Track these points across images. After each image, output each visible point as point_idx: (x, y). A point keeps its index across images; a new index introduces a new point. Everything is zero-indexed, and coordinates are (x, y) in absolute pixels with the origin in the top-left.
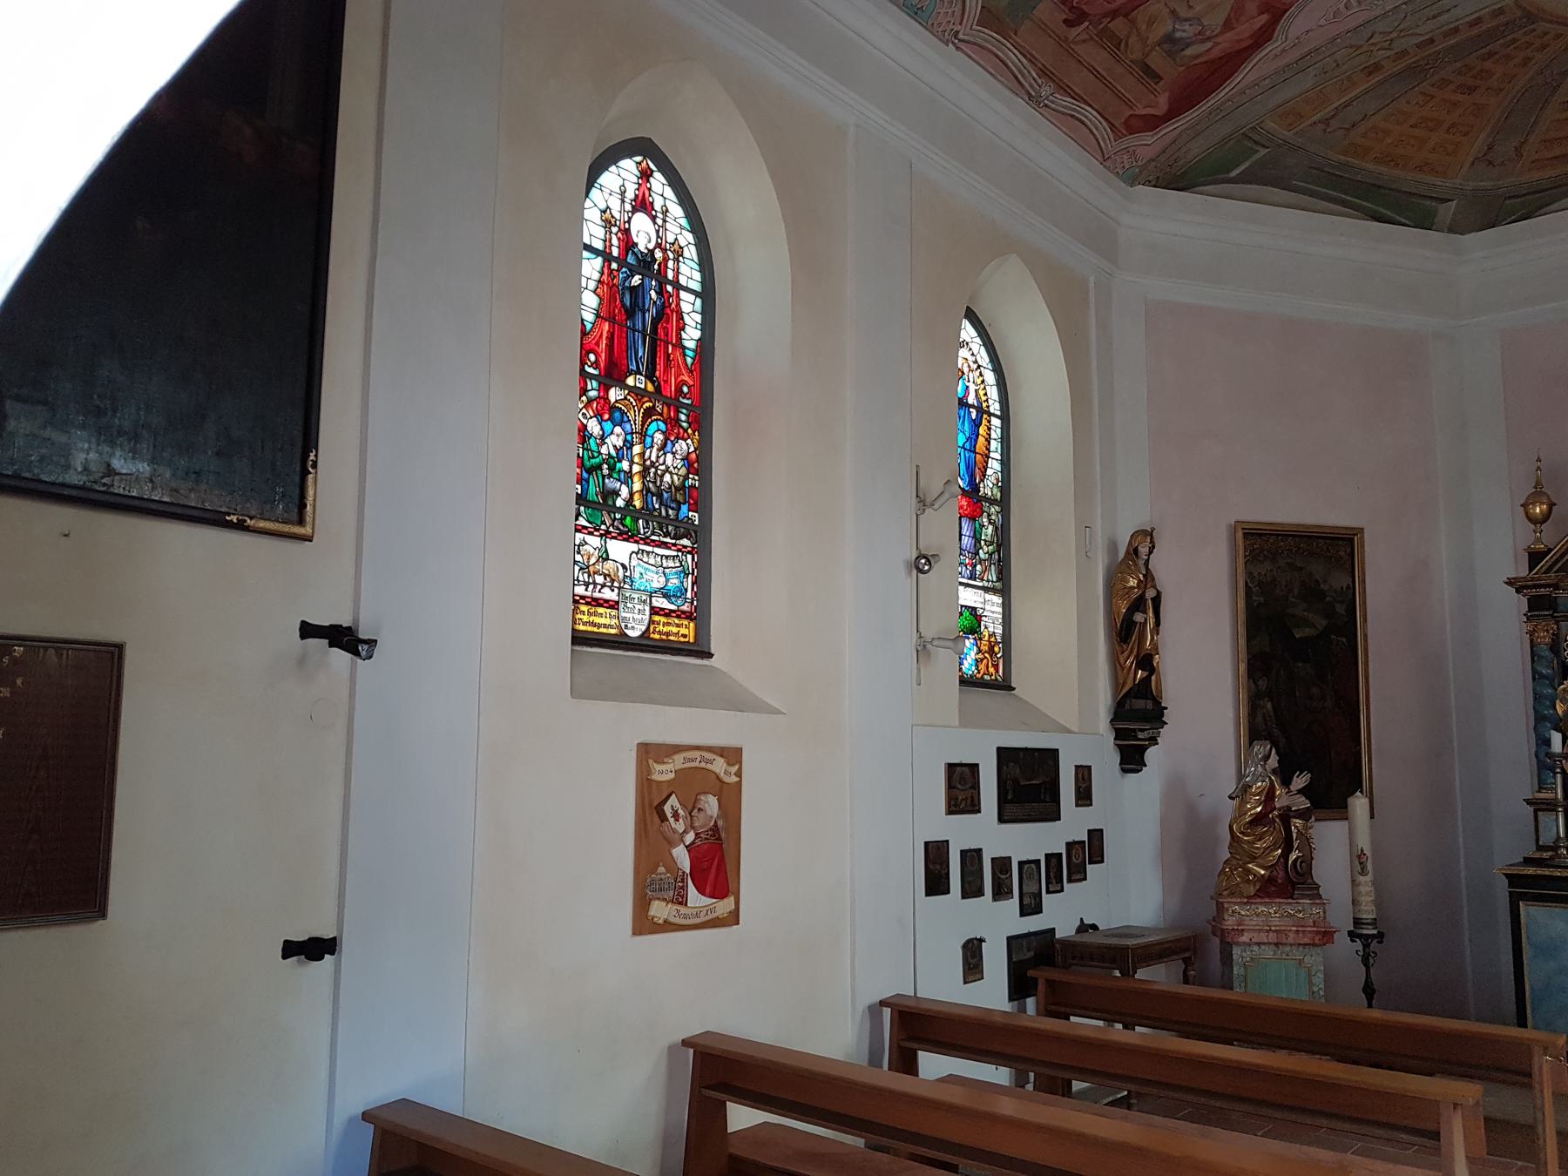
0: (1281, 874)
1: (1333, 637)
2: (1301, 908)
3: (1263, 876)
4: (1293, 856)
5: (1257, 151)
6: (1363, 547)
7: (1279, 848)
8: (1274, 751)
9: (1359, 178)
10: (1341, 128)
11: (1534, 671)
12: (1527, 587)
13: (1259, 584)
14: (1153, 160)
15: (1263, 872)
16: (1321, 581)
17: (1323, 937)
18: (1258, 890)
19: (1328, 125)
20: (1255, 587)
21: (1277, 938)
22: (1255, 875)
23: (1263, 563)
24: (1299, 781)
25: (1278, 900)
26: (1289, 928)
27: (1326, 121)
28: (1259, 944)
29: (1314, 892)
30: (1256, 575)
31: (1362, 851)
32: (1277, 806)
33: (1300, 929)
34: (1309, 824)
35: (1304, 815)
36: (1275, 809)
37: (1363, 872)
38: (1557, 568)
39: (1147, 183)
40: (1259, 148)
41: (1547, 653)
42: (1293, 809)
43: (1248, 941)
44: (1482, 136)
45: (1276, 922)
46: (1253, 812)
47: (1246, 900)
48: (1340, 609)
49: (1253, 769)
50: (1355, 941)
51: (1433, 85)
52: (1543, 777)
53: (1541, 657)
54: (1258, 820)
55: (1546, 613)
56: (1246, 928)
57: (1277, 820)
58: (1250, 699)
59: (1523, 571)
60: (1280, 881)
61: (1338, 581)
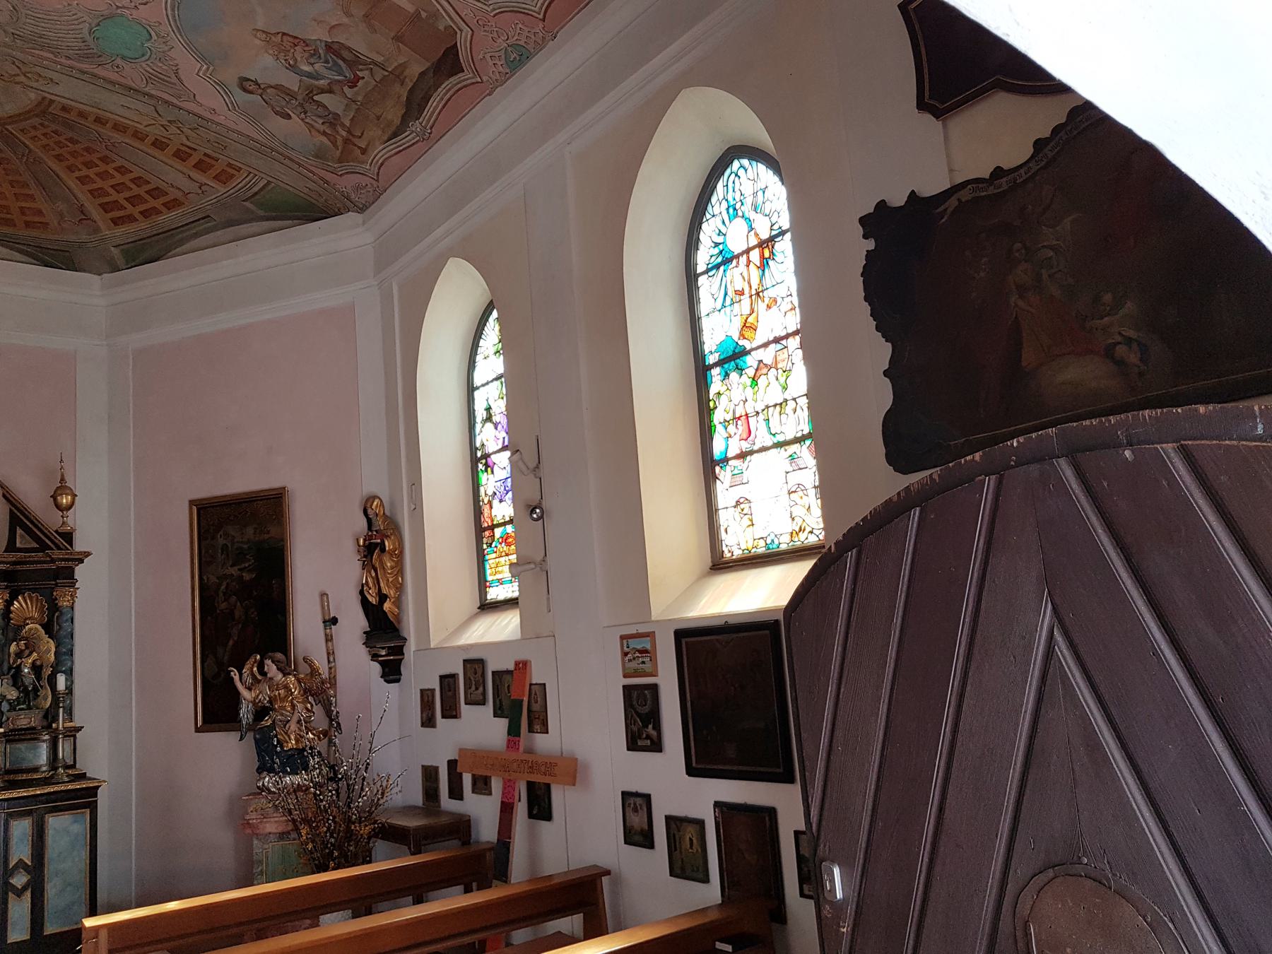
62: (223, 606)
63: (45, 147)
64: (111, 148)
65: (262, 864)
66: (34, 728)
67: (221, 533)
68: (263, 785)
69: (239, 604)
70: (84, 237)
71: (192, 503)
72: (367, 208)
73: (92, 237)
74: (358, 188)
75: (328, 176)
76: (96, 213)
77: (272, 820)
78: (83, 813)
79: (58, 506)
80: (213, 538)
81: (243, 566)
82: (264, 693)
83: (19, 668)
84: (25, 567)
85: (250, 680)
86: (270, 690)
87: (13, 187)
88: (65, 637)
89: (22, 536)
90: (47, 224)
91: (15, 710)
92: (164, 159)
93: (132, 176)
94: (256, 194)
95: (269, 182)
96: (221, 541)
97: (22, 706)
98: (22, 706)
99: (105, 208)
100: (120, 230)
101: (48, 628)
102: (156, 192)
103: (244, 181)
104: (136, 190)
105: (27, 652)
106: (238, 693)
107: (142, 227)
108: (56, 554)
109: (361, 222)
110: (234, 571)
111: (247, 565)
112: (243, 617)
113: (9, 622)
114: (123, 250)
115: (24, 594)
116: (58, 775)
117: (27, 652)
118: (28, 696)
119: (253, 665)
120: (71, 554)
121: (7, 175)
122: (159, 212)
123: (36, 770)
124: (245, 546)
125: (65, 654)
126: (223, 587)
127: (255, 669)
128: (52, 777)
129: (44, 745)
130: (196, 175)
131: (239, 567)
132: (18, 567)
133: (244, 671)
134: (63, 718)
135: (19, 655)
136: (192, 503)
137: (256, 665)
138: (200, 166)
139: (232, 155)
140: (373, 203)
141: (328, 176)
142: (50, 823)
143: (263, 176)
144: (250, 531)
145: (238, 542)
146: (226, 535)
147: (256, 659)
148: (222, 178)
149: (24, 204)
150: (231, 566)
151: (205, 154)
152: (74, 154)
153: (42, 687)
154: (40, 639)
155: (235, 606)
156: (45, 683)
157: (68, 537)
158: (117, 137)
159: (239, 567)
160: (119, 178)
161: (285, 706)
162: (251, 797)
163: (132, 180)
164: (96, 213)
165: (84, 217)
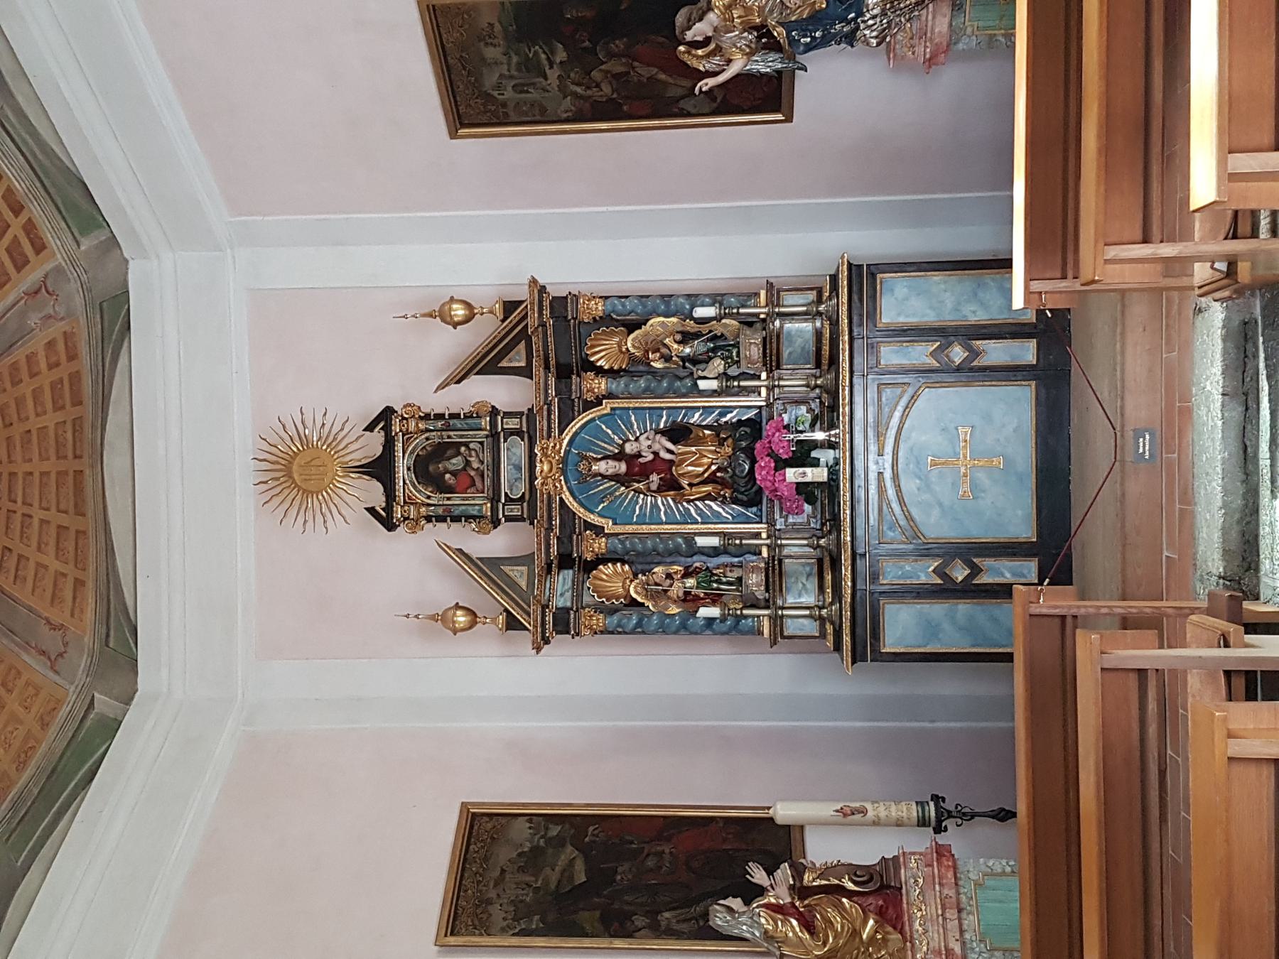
0: (871, 900)
1: (587, 839)
2: (913, 878)
3: (876, 922)
4: (850, 886)
6: (484, 804)
7: (840, 901)
8: (721, 902)
9: (36, 791)
11: (633, 632)
12: (543, 632)
13: (518, 921)
15: (871, 922)
16: (520, 850)
17: (944, 856)
18: (895, 928)
20: (519, 924)
21: (950, 908)
22: (876, 932)
23: (491, 915)
24: (758, 875)
25: (905, 906)
26: (938, 893)
28: (962, 932)
29: (890, 865)
30: (505, 923)
31: (837, 811)
32: (788, 900)
33: (937, 880)
34: (810, 865)
35: (798, 871)
36: (793, 904)
37: (863, 811)
38: (525, 607)
41: (615, 618)
42: (792, 882)
43: (959, 943)
44: (25, 657)
45: (933, 909)
46: (798, 929)
47: (908, 944)
48: (554, 831)
49: (744, 927)
50: (946, 827)
52: (746, 629)
53: (619, 625)
54: (808, 925)
55: (572, 616)
56: (943, 944)
57: (806, 902)
58: (658, 937)
59: (524, 640)
60: (881, 902)
61: (521, 831)
62: (607, 89)
65: (995, 35)
66: (764, 339)
67: (495, 93)
68: (876, 37)
69: (603, 67)
70: (74, 286)
71: (453, 135)
73: (71, 276)
76: (32, 277)
77: (930, 24)
78: (881, 282)
79: (467, 320)
80: (504, 105)
81: (545, 62)
82: (738, 40)
83: (683, 359)
84: (552, 355)
85: (716, 60)
86: (734, 31)
87: (21, 381)
88: (644, 306)
89: (510, 361)
91: (738, 362)
96: (509, 94)
97: (734, 354)
98: (734, 354)
99: (21, 264)
100: (49, 238)
101: (632, 327)
105: (664, 350)
106: (738, 76)
107: (38, 211)
108: (533, 321)
110: (553, 74)
111: (543, 56)
112: (624, 60)
113: (624, 370)
115: (587, 355)
116: (827, 311)
117: (664, 350)
118: (721, 346)
119: (694, 56)
120: (532, 303)
123: (818, 334)
124: (515, 59)
125: (666, 303)
126: (579, 90)
127: (700, 52)
128: (829, 319)
129: (788, 326)
131: (547, 68)
132: (552, 362)
133: (701, 68)
134: (755, 306)
135: (668, 359)
136: (453, 135)
137: (693, 52)
142: (888, 321)
144: (491, 53)
145: (509, 71)
146: (498, 87)
147: (684, 52)
149: (43, 365)
150: (546, 79)
153: (710, 331)
154: (647, 334)
155: (607, 72)
156: (704, 328)
157: (510, 307)
159: (547, 68)
161: (759, 7)
162: (891, 56)
164: (32, 277)
165: (43, 290)
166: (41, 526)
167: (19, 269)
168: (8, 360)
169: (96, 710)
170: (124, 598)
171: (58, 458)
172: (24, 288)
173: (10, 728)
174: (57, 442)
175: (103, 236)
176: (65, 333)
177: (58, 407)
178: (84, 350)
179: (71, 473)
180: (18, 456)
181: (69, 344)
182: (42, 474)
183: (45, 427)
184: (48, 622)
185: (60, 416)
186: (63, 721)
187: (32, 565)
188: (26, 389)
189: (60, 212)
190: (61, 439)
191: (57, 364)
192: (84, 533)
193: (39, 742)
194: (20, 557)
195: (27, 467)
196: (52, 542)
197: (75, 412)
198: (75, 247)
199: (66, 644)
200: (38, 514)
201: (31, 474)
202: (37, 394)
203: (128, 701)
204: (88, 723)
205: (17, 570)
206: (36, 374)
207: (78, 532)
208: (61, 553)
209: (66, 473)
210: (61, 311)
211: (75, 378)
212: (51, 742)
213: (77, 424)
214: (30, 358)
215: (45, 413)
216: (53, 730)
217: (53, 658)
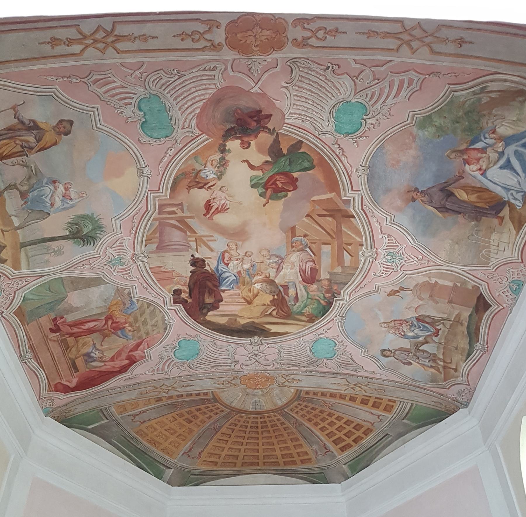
5: (103, 420)
9: (139, 447)
10: (139, 421)
14: (60, 407)
19: (135, 418)
27: (134, 416)
39: (53, 417)
40: (104, 418)
51: (177, 415)
63: (303, 416)
64: (331, 407)
70: (329, 462)
72: (469, 404)
73: (332, 461)
74: (460, 393)
75: (442, 391)
76: (331, 446)
87: (292, 442)
90: (311, 459)
92: (357, 406)
93: (344, 420)
94: (408, 413)
95: (412, 404)
99: (336, 442)
100: (346, 453)
102: (358, 427)
103: (399, 408)
104: (348, 428)
107: (356, 449)
109: (468, 413)
114: (349, 465)
121: (289, 436)
122: (362, 438)
130: (375, 411)
138: (376, 405)
139: (389, 394)
140: (471, 399)
141: (442, 391)
143: (408, 401)
148: (388, 409)
149: (299, 450)
151: (376, 398)
152: (316, 416)
158: (333, 401)
160: (339, 424)
163: (345, 423)
164: (331, 446)
166: (238, 449)
167: (334, 441)
168: (299, 437)
169: (166, 470)
170: (209, 481)
171: (264, 456)
172: (326, 443)
173: (163, 437)
174: (270, 455)
175: (349, 473)
176: (311, 459)
177: (283, 456)
178: (305, 466)
179: (258, 461)
180: (265, 440)
181: (307, 461)
182: (258, 450)
183: (275, 451)
184: (202, 451)
185: (279, 456)
186: (165, 458)
187: (224, 445)
188: (290, 444)
189: (356, 457)
190: (271, 457)
191: (299, 456)
192: (235, 466)
193: (157, 448)
194: (227, 441)
195: (260, 444)
196: (232, 453)
197: (281, 463)
198: (344, 463)
199: (193, 458)
200: (243, 448)
201: (258, 446)
202: (288, 448)
203: (168, 483)
204: (162, 467)
205: (222, 440)
206: (295, 448)
207: (236, 463)
208: (228, 457)
209: (258, 459)
210: (319, 457)
211: (294, 463)
212: (157, 453)
213: (277, 464)
214: (301, 445)
215: (281, 451)
216: (162, 454)
217: (188, 453)
